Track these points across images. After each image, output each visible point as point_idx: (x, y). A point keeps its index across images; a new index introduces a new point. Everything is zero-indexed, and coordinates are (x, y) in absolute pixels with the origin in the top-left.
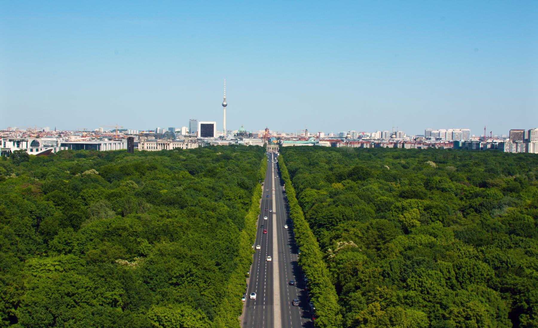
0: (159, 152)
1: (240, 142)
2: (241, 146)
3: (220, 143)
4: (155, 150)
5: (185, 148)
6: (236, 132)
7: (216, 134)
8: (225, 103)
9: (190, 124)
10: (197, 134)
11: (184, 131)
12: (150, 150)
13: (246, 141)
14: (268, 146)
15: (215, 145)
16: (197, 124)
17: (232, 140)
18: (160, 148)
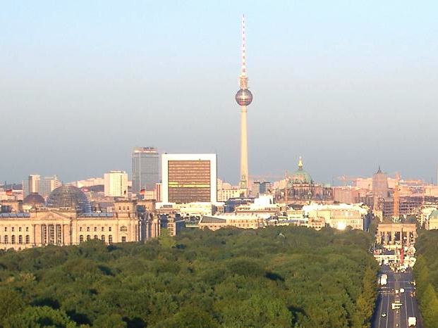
0: (35, 252)
1: (295, 217)
2: (297, 231)
3: (230, 219)
4: (23, 247)
5: (116, 240)
6: (282, 184)
7: (219, 192)
8: (244, 97)
9: (135, 161)
10: (159, 194)
11: (115, 184)
12: (8, 247)
13: (314, 213)
14: (382, 229)
15: (214, 227)
16: (157, 160)
17: (269, 210)
18: (37, 240)
